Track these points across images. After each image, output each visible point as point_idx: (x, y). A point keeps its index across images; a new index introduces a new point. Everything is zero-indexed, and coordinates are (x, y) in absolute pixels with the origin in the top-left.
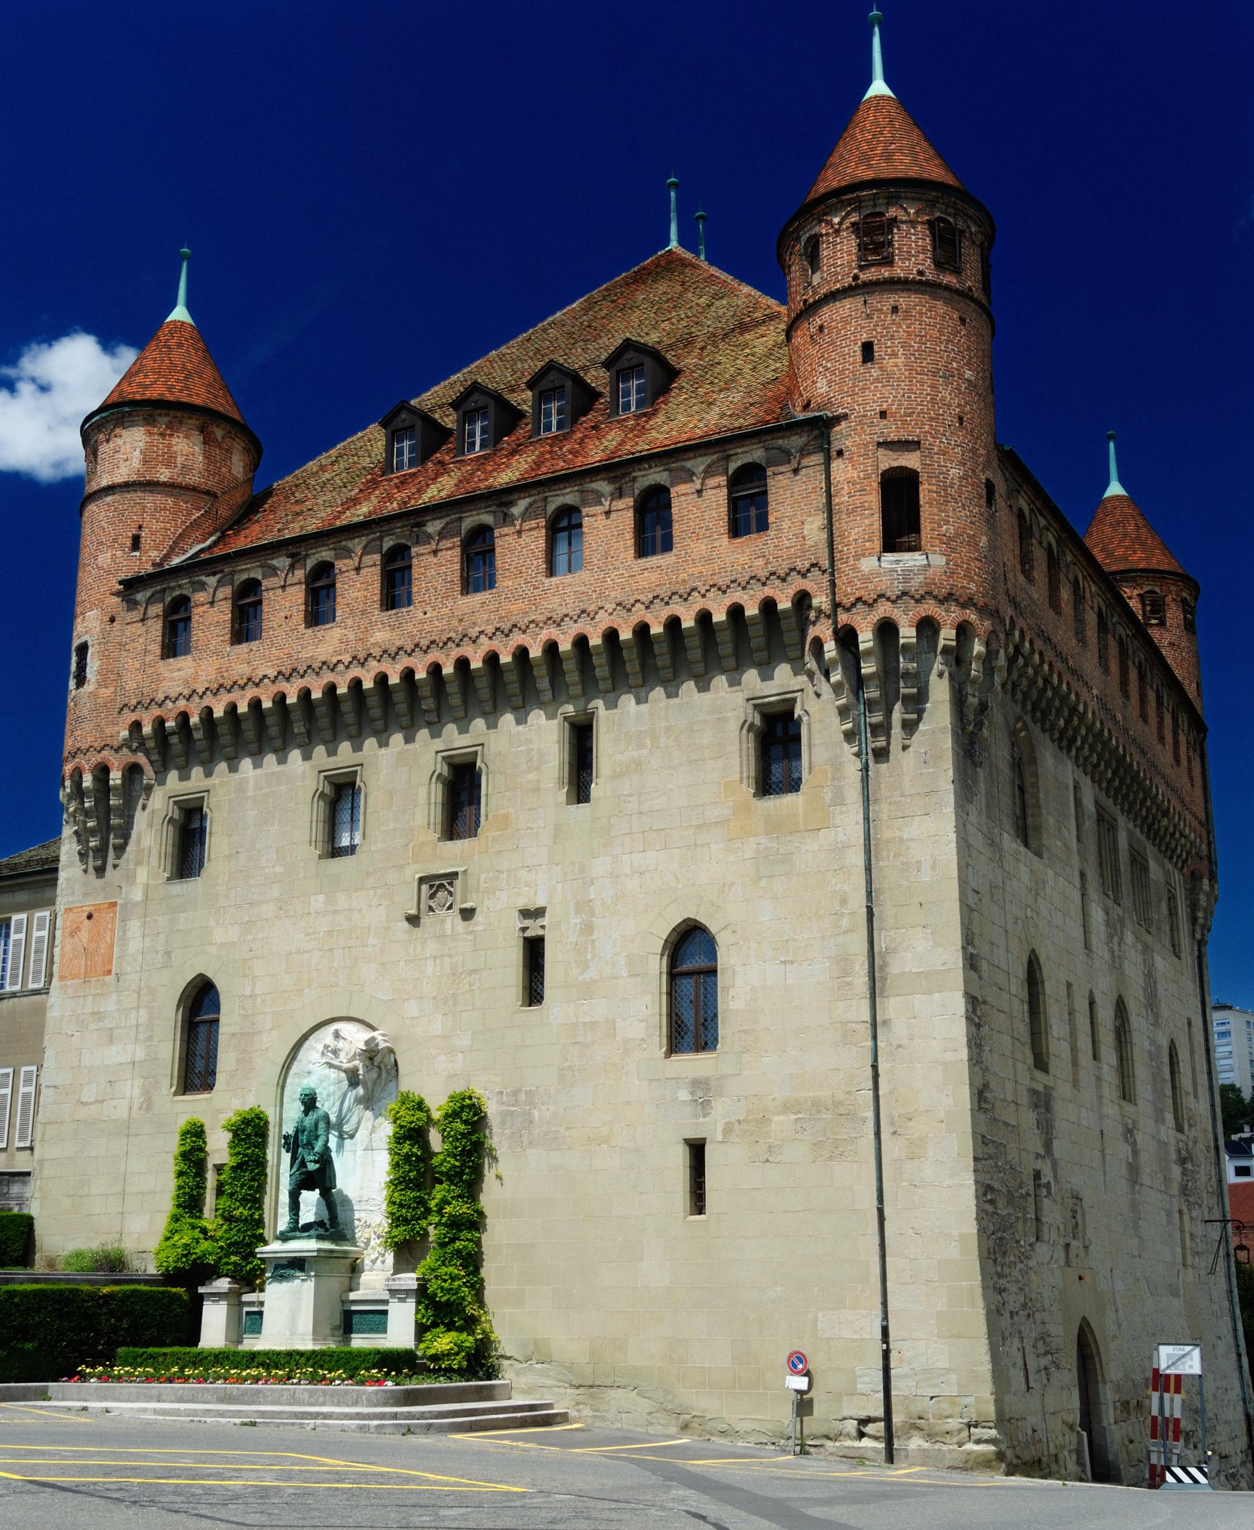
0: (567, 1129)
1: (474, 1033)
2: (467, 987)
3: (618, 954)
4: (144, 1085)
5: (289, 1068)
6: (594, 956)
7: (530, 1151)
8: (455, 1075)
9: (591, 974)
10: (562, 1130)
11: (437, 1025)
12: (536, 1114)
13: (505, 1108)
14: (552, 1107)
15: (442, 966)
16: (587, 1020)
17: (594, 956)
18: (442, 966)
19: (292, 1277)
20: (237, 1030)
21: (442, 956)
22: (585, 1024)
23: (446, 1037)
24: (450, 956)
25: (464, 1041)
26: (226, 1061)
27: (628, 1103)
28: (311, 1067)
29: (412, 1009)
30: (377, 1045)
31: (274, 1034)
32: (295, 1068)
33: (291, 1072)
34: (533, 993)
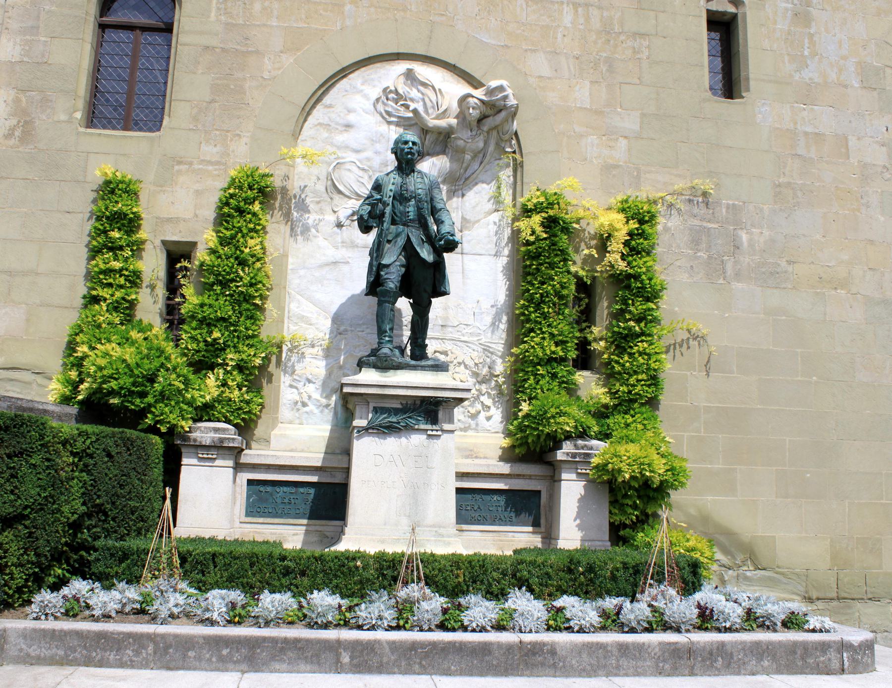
0: (789, 262)
1: (643, 115)
2: (629, 52)
3: (844, 58)
4: (17, 101)
5: (309, 114)
6: (814, 54)
7: (737, 286)
8: (616, 167)
9: (811, 74)
10: (783, 264)
11: (583, 94)
12: (744, 237)
13: (696, 222)
14: (766, 233)
15: (588, 19)
16: (809, 129)
17: (814, 54)
18: (588, 19)
19: (409, 429)
20: (214, 42)
21: (587, 5)
22: (806, 134)
23: (599, 113)
24: (600, 8)
25: (630, 123)
26: (190, 81)
27: (871, 242)
28: (352, 118)
29: (539, 65)
30: (506, 98)
31: (288, 60)
32: (318, 114)
33: (311, 119)
34: (729, 83)
